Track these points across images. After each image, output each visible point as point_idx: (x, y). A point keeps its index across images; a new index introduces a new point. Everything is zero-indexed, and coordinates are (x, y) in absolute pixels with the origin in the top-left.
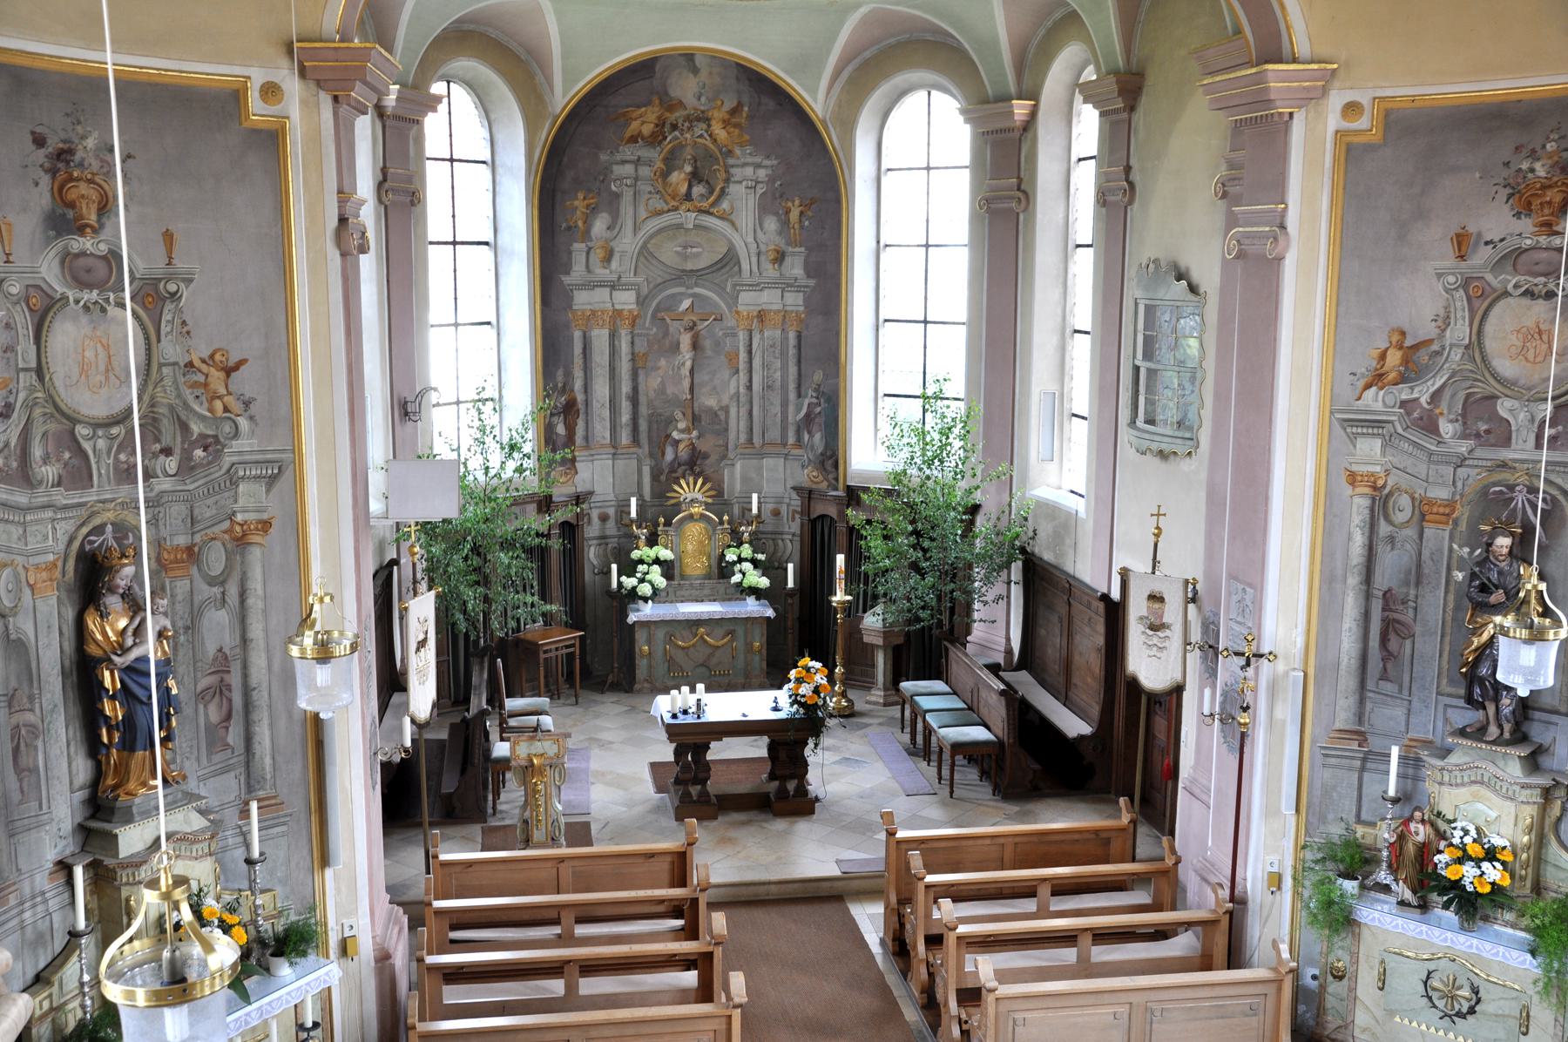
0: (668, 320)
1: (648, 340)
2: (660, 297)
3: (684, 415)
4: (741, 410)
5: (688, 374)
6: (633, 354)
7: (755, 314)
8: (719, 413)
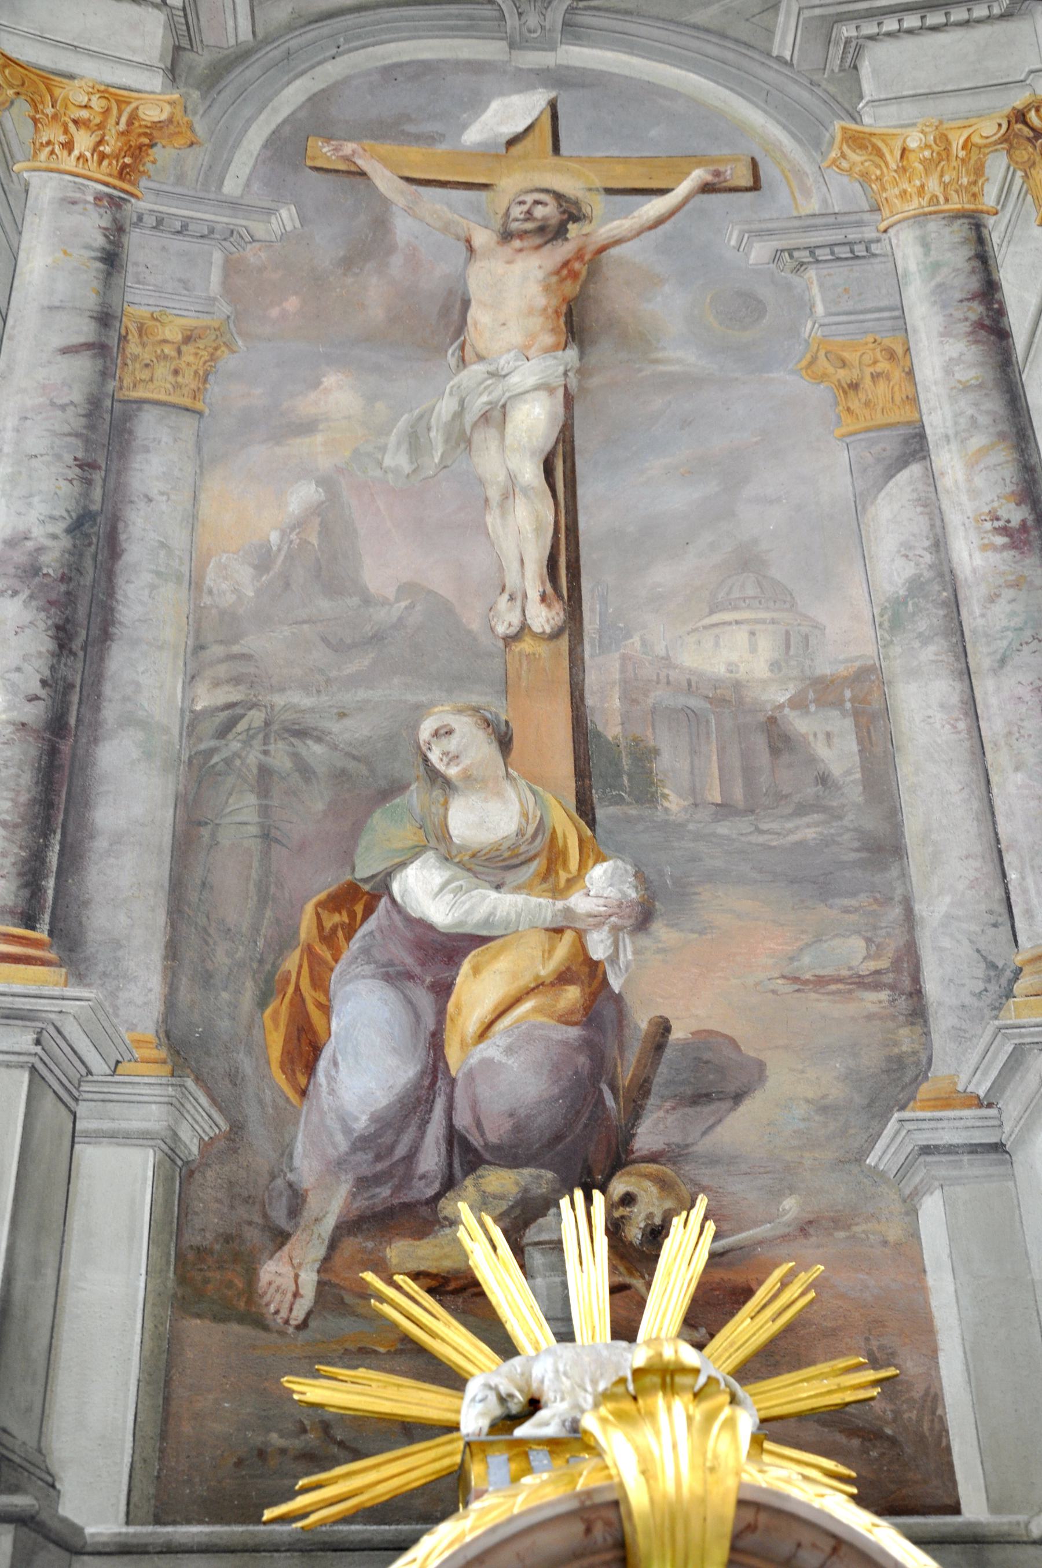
0: (384, 180)
1: (231, 267)
2: (332, 71)
3: (505, 743)
4: (986, 688)
5: (531, 473)
6: (105, 319)
7: (989, 129)
8: (800, 725)
